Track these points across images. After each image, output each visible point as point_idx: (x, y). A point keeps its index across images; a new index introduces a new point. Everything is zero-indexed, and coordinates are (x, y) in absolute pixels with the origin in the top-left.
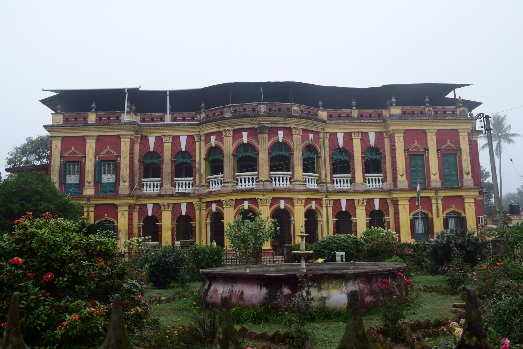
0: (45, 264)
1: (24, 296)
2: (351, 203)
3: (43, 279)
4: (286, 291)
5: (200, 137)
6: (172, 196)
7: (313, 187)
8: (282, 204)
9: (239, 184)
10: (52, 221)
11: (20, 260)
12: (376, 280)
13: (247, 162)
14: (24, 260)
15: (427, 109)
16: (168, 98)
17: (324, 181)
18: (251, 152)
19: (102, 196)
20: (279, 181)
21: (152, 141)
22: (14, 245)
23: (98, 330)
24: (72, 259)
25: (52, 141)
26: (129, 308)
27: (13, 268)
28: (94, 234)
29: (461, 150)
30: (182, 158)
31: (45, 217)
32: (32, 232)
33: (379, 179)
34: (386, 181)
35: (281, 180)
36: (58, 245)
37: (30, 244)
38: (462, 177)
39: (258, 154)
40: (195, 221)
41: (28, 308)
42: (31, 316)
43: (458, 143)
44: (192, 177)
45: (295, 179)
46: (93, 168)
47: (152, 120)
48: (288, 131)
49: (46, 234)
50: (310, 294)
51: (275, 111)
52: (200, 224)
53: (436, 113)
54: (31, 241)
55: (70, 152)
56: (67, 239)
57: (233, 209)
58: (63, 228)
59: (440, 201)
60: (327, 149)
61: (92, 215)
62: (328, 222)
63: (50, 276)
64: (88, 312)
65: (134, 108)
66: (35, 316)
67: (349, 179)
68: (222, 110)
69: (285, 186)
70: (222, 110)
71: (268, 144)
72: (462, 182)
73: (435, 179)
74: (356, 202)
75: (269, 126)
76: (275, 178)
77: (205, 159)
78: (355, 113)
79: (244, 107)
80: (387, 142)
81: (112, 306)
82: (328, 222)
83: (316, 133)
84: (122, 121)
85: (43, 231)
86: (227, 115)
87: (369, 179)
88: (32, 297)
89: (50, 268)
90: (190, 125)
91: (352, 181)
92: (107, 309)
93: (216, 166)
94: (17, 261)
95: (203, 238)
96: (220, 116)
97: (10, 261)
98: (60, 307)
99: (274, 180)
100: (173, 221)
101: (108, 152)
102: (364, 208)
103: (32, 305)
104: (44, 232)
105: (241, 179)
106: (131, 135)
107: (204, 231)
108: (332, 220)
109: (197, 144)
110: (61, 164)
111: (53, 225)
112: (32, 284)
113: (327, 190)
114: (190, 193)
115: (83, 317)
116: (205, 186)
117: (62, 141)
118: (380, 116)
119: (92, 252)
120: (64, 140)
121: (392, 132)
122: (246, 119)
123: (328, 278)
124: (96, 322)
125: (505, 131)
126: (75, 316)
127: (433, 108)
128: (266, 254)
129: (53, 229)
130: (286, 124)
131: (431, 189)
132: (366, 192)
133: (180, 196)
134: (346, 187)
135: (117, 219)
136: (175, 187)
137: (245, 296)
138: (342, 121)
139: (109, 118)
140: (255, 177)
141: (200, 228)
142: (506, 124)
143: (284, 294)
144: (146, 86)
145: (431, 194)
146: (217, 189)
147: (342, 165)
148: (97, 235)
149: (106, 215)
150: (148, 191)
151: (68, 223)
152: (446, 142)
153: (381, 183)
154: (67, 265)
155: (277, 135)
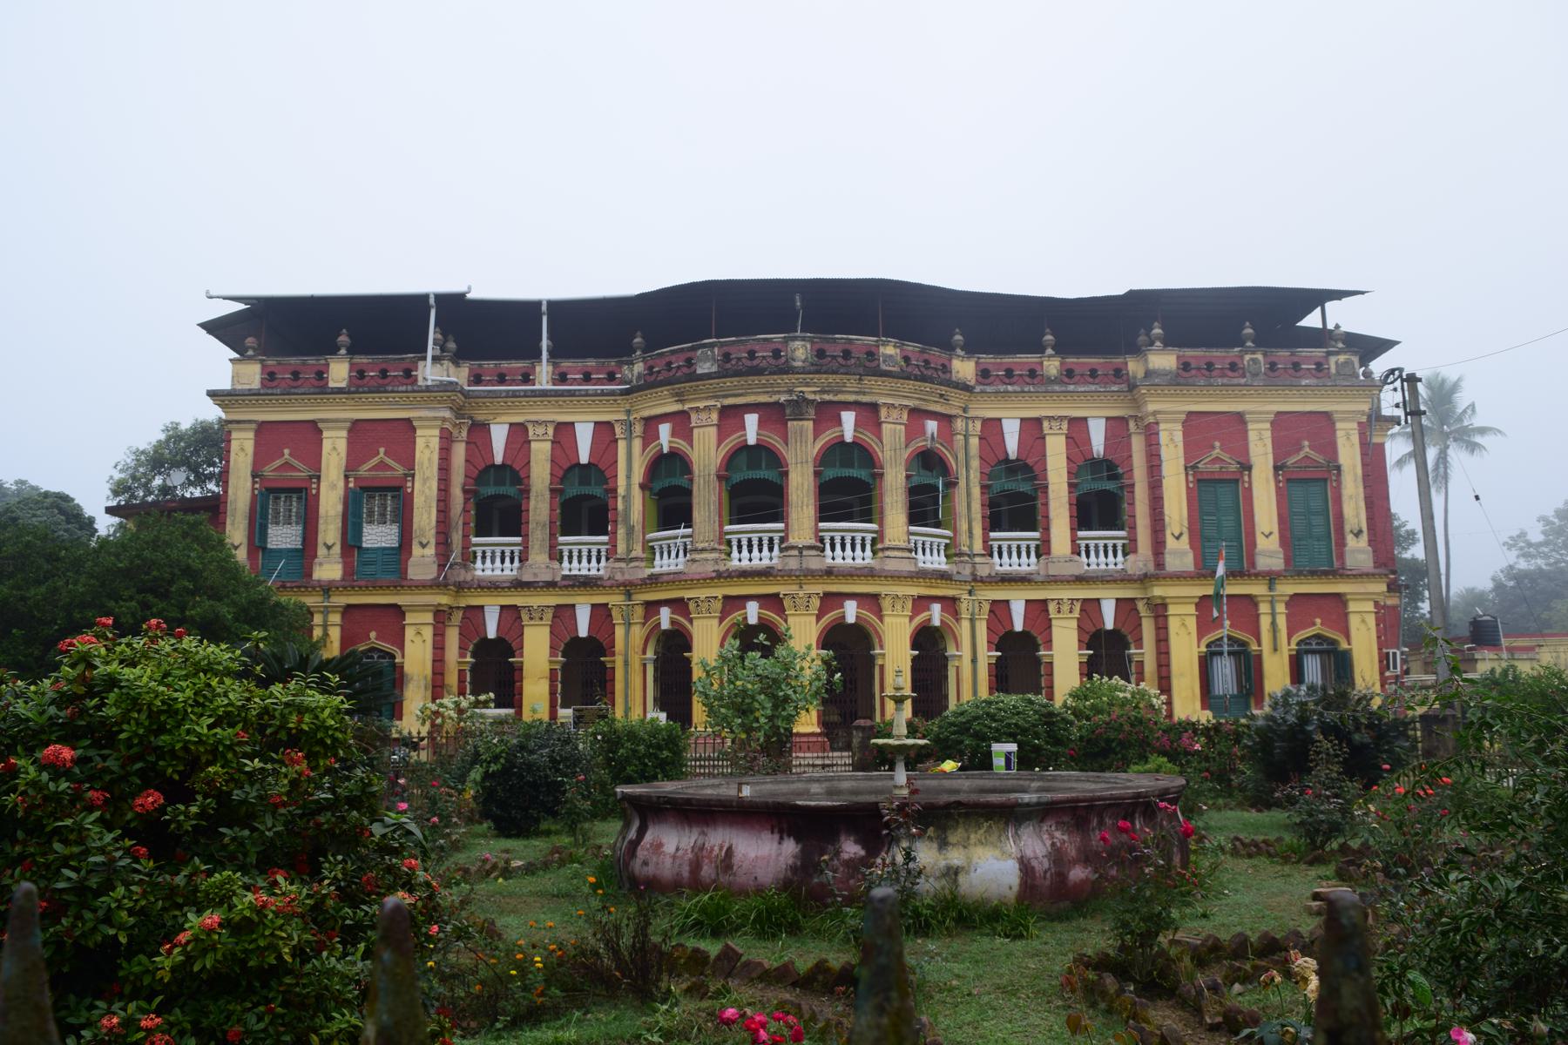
0: (139, 765)
1: (72, 857)
2: (1037, 609)
3: (132, 808)
4: (851, 849)
5: (629, 426)
6: (551, 585)
7: (936, 566)
8: (851, 611)
9: (735, 554)
10: (165, 645)
11: (67, 753)
12: (1101, 823)
13: (755, 495)
14: (79, 752)
15: (1247, 357)
16: (545, 319)
17: (965, 549)
18: (767, 468)
19: (363, 583)
20: (843, 549)
21: (499, 436)
22: (52, 710)
23: (280, 957)
24: (216, 753)
25: (229, 432)
26: (378, 894)
27: (45, 776)
28: (285, 682)
29: (1338, 468)
30: (581, 483)
31: (146, 631)
32: (109, 674)
33: (1115, 546)
34: (1135, 551)
35: (848, 547)
36: (176, 712)
37: (98, 708)
38: (1342, 543)
39: (786, 474)
40: (613, 654)
41: (80, 889)
42: (88, 915)
43: (1331, 449)
44: (606, 533)
45: (887, 543)
46: (340, 508)
47: (502, 380)
48: (870, 413)
49: (145, 679)
50: (914, 859)
51: (834, 357)
52: (626, 663)
53: (1272, 366)
54: (102, 699)
55: (278, 463)
56: (205, 696)
57: (716, 622)
58: (196, 664)
59: (1281, 608)
60: (975, 463)
61: (335, 634)
62: (974, 661)
63: (152, 799)
64: (251, 906)
65: (452, 345)
66: (101, 913)
67: (1033, 544)
68: (689, 354)
69: (859, 561)
70: (689, 354)
71: (814, 448)
72: (1341, 556)
73: (1268, 548)
74: (1052, 607)
75: (818, 398)
76: (832, 539)
77: (642, 487)
78: (1052, 366)
79: (749, 347)
80: (1137, 445)
81: (326, 888)
82: (974, 661)
83: (946, 419)
84: (420, 382)
85: (137, 671)
86: (704, 368)
87: (1087, 547)
88: (92, 859)
89: (151, 779)
90: (603, 393)
91: (1043, 550)
92: (309, 896)
93: (672, 507)
94: (57, 754)
95: (635, 702)
96: (685, 370)
97: (38, 755)
98: (173, 890)
99: (828, 547)
100: (552, 654)
101: (382, 466)
102: (1074, 624)
103: (93, 882)
104: (141, 676)
105: (739, 541)
106: (444, 420)
107: (636, 680)
108: (987, 656)
109: (622, 445)
110: (254, 497)
111: (168, 655)
112: (100, 821)
113: (973, 574)
114: (600, 578)
115: (237, 918)
116: (642, 560)
117: (258, 433)
118: (1119, 373)
119: (276, 733)
120: (262, 429)
121: (1151, 419)
122: (756, 380)
123: (967, 816)
124: (272, 935)
125: (1460, 419)
126: (212, 917)
127: (1265, 355)
128: (805, 746)
129: (165, 666)
130: (864, 394)
131: (1257, 575)
132: (1081, 580)
133: (573, 586)
134: (1025, 568)
135: (402, 648)
136: (561, 561)
137: (736, 860)
138: (1017, 388)
139: (384, 373)
140: (776, 537)
141: (626, 672)
142: (1462, 400)
143: (845, 856)
144: (483, 289)
145: (1257, 589)
146: (673, 568)
147: (1014, 507)
148: (292, 685)
149: (373, 635)
150: (488, 573)
151: (213, 648)
152: (1301, 449)
153: (1120, 557)
154: (203, 770)
155: (839, 422)
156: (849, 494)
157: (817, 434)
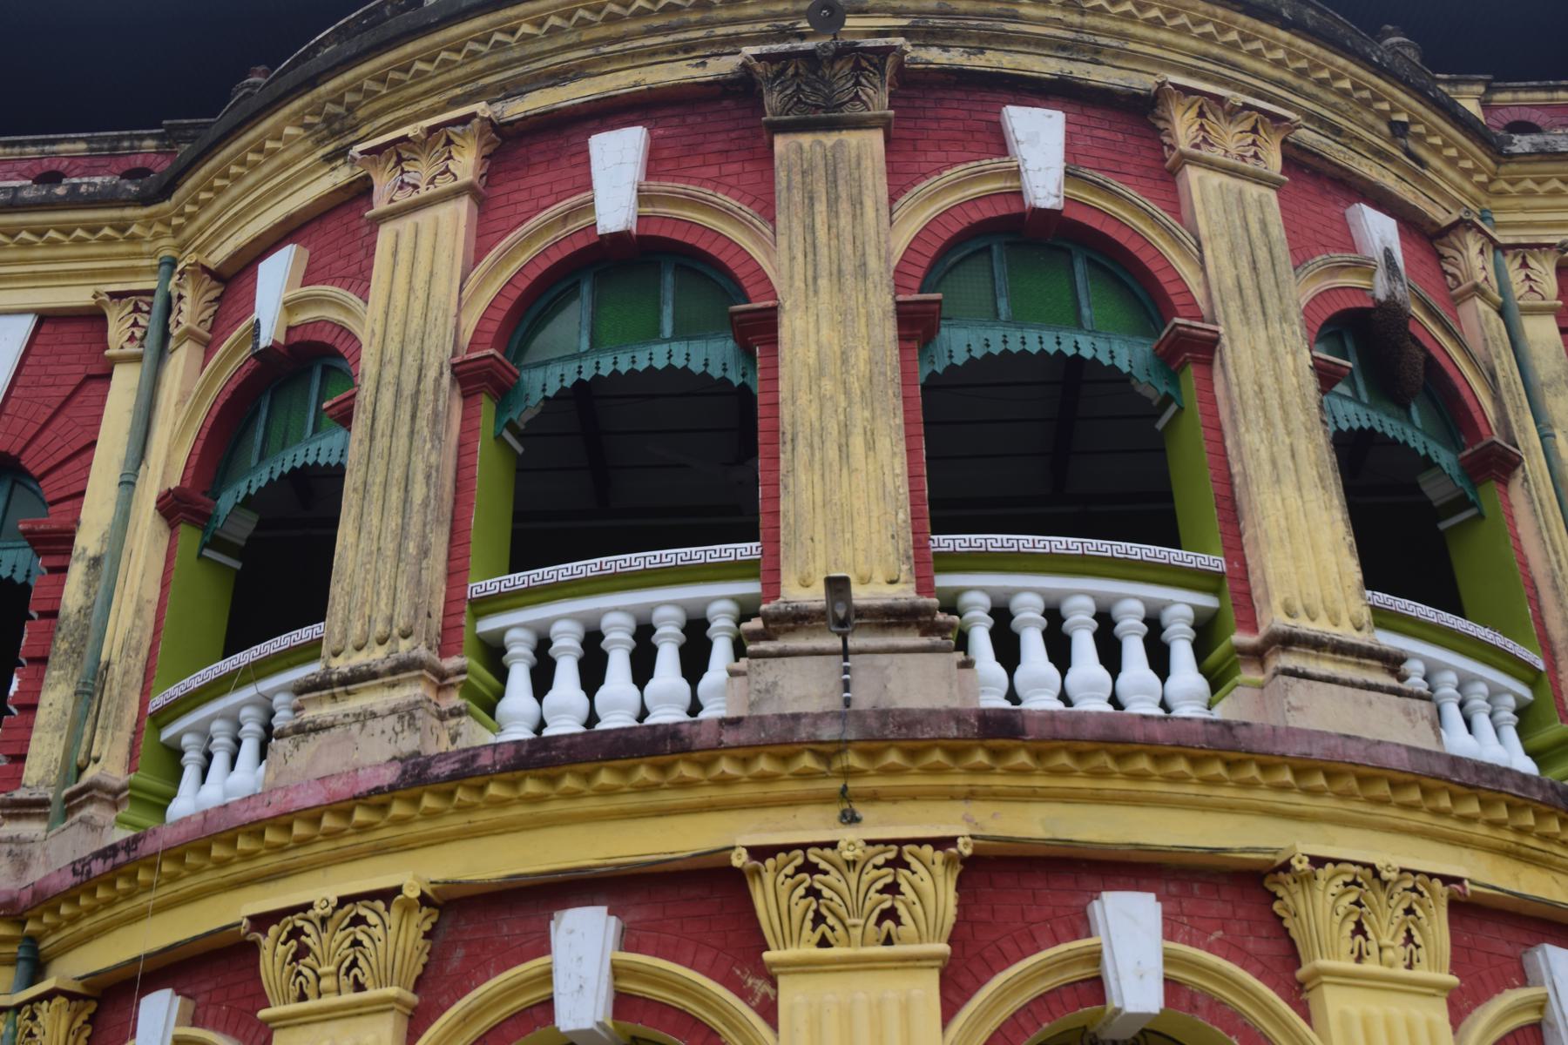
13: (630, 451)
109: (124, 385)
130: (1095, 54)
155: (999, 142)
156: (1057, 438)
157: (900, 181)
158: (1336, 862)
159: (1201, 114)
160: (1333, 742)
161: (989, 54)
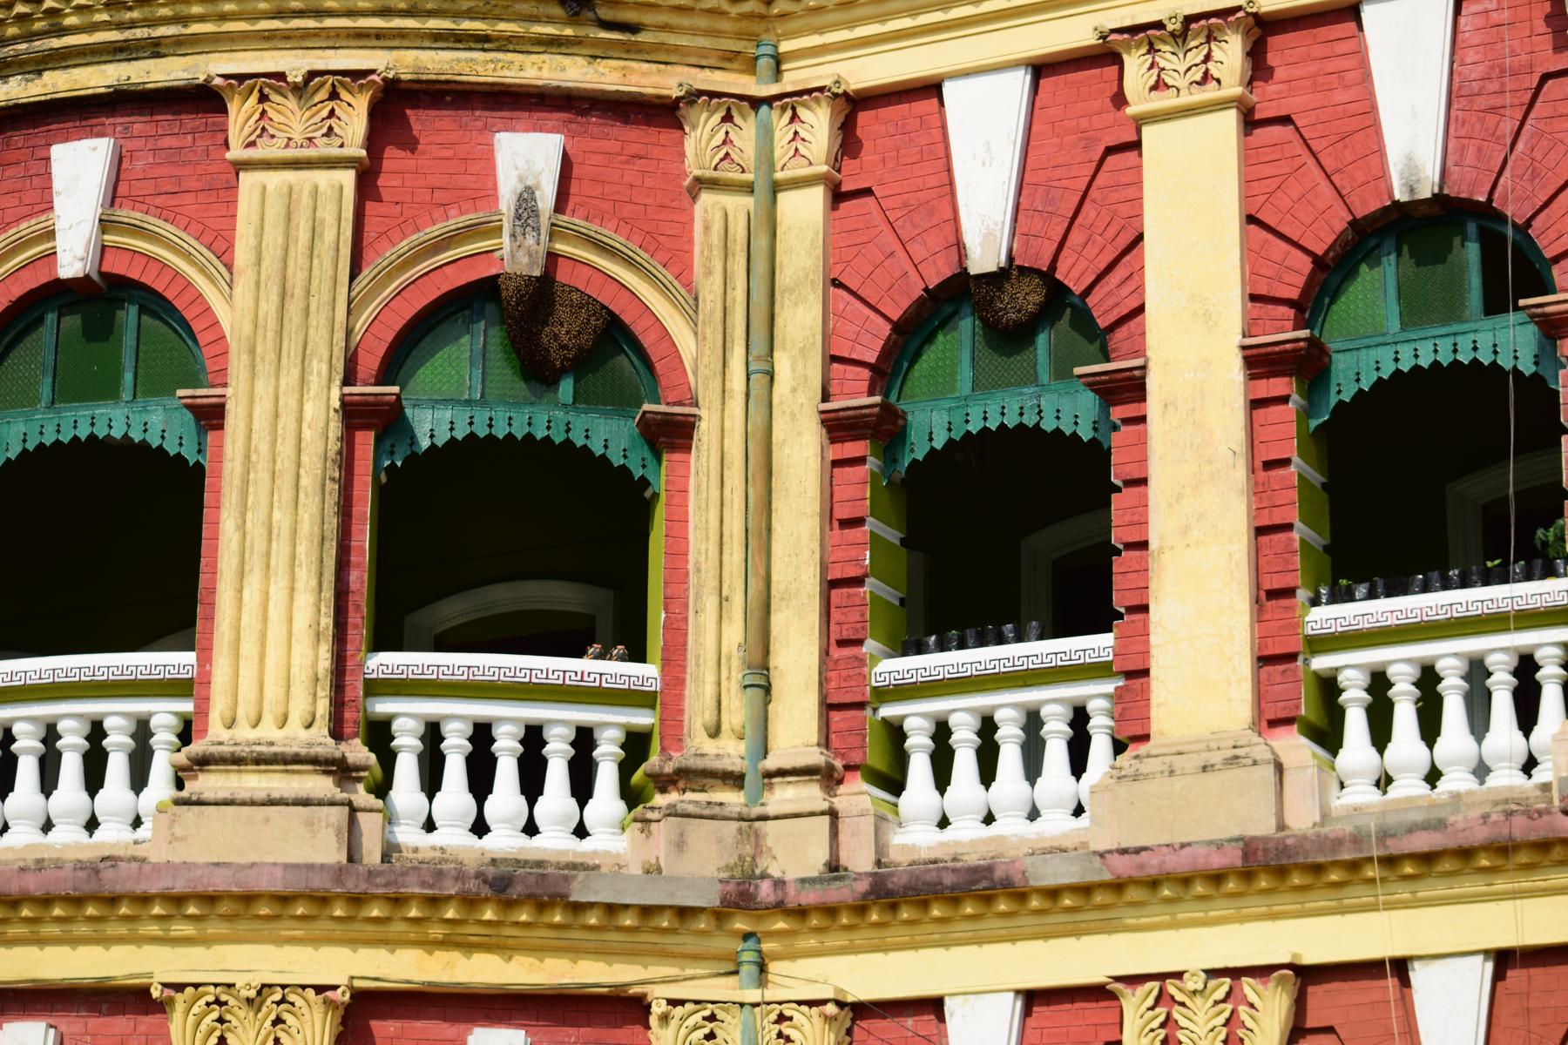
17: (731, 752)
60: (802, 320)
130: (156, 49)
132: (1270, 868)
158: (196, 986)
159: (263, 98)
160: (199, 872)
161: (47, 75)
